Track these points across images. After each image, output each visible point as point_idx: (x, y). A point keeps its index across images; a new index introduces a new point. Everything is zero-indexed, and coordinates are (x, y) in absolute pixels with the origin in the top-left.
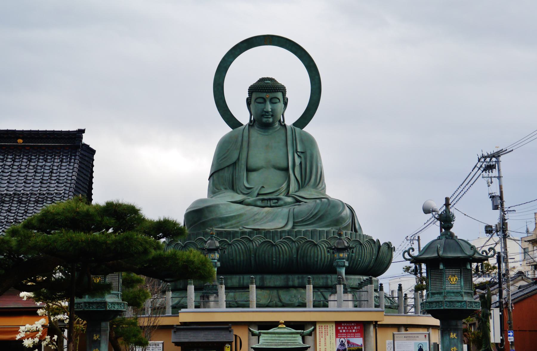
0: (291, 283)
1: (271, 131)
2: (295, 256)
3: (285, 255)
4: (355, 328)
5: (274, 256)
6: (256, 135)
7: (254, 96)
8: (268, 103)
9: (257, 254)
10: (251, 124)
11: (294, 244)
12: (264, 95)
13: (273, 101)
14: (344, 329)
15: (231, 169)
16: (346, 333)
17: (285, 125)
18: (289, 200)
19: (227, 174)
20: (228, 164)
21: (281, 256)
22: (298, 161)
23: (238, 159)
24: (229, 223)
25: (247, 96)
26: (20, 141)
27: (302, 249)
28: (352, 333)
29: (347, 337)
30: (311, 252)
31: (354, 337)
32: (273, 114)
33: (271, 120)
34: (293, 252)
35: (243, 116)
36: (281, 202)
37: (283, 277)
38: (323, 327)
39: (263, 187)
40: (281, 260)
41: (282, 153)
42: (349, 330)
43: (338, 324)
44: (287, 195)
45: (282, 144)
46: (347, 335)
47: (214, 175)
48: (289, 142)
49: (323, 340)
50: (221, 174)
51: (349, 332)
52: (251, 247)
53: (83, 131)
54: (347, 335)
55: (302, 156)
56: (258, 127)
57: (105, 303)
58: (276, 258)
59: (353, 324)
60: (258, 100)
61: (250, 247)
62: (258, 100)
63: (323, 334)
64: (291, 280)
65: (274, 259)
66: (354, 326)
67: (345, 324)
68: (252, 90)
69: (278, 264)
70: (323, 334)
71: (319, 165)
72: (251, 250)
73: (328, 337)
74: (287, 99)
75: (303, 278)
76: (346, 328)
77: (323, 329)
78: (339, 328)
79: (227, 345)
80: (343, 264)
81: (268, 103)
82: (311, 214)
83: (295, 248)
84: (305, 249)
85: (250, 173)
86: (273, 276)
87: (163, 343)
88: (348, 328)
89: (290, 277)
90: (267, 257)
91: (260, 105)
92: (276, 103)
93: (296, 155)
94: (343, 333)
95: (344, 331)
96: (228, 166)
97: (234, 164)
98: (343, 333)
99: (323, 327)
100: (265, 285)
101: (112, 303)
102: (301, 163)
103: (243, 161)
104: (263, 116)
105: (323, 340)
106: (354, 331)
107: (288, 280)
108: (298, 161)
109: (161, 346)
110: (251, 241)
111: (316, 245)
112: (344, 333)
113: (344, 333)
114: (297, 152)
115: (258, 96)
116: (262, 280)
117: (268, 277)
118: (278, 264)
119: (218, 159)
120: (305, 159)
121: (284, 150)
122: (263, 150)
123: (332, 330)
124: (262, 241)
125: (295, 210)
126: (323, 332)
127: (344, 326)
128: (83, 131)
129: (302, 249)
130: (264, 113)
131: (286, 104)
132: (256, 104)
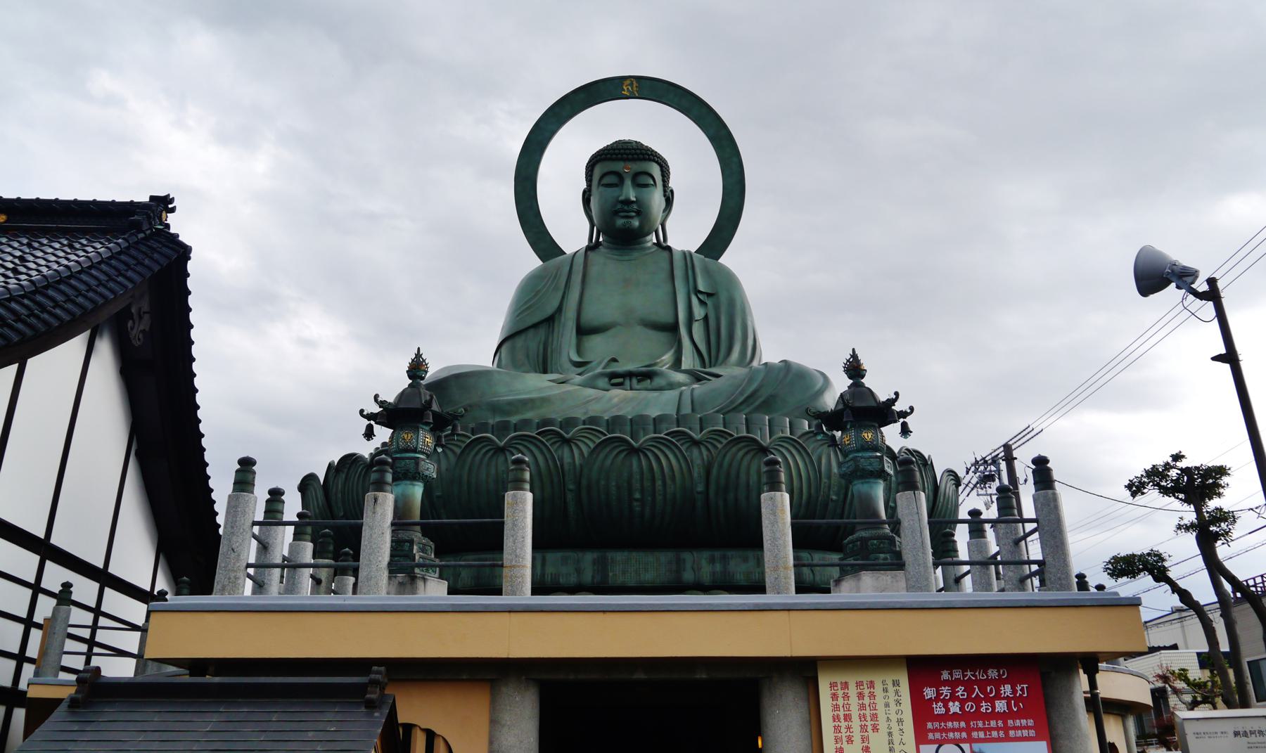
0: (688, 576)
1: (636, 254)
2: (700, 488)
3: (669, 482)
4: (1007, 690)
5: (637, 485)
6: (606, 265)
8: (628, 182)
9: (584, 482)
10: (592, 247)
11: (695, 452)
12: (618, 166)
14: (954, 698)
15: (542, 332)
16: (963, 716)
17: (669, 249)
18: (680, 377)
19: (533, 342)
20: (536, 319)
21: (659, 483)
23: (560, 310)
27: (721, 465)
28: (994, 715)
29: (970, 740)
30: (748, 474)
31: (1008, 739)
32: (641, 210)
33: (636, 223)
34: (695, 475)
36: (658, 381)
37: (665, 557)
38: (853, 691)
39: (614, 360)
40: (659, 498)
41: (662, 293)
42: (977, 701)
43: (923, 669)
45: (663, 276)
46: (969, 730)
47: (504, 349)
48: (679, 273)
50: (519, 342)
51: (978, 715)
52: (567, 459)
53: (163, 204)
54: (969, 730)
55: (709, 302)
56: (608, 248)
58: (642, 491)
59: (993, 673)
60: (605, 181)
61: (561, 460)
62: (606, 180)
63: (856, 723)
64: (688, 565)
65: (637, 496)
66: (998, 683)
67: (957, 674)
69: (647, 510)
70: (856, 723)
71: (749, 323)
72: (566, 467)
74: (672, 192)
75: (724, 559)
76: (960, 691)
77: (854, 701)
78: (929, 693)
80: (876, 466)
81: (628, 182)
82: (741, 394)
83: (698, 461)
84: (728, 474)
85: (585, 338)
86: (634, 554)
88: (969, 690)
89: (687, 556)
90: (613, 490)
91: (610, 190)
92: (646, 186)
93: (695, 301)
94: (947, 717)
95: (955, 707)
96: (535, 326)
97: (550, 321)
98: (947, 717)
99: (853, 691)
100: (611, 582)
102: (706, 318)
106: (1001, 706)
107: (680, 563)
108: (699, 312)
110: (567, 442)
112: (955, 717)
113: (955, 717)
114: (697, 292)
115: (606, 170)
116: (602, 565)
117: (619, 556)
118: (647, 510)
119: (516, 310)
120: (717, 308)
121: (668, 288)
122: (616, 293)
123: (893, 699)
124: (598, 441)
125: (696, 393)
127: (953, 684)
128: (163, 204)
129: (721, 465)
130: (619, 206)
132: (601, 189)
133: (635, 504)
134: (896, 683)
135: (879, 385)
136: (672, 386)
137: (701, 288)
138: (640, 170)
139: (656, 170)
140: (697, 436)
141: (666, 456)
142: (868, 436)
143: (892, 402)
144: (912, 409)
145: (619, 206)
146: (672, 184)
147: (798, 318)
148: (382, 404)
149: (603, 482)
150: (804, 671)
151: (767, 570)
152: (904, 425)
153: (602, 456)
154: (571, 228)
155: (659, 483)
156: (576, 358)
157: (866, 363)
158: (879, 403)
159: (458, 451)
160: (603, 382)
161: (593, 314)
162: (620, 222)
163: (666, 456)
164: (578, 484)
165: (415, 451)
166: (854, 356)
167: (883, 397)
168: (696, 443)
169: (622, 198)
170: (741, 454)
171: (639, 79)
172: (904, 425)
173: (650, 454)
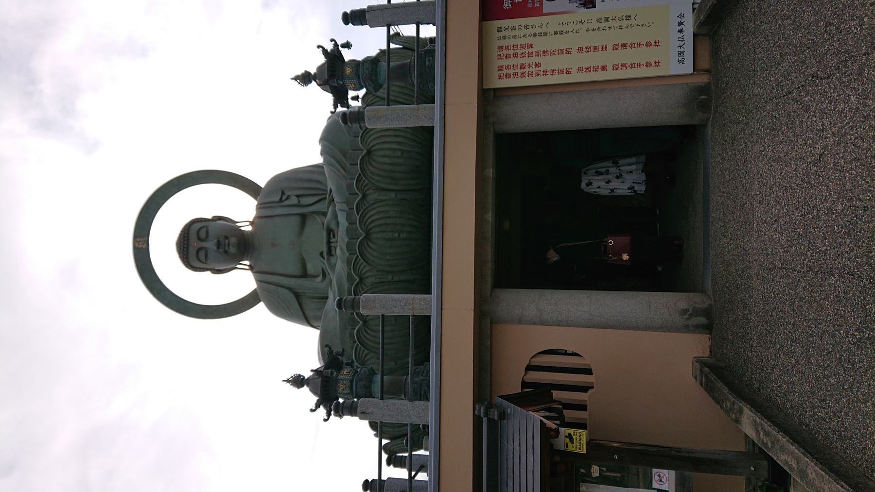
2: (393, 195)
8: (204, 244)
9: (387, 269)
12: (192, 251)
20: (296, 304)
21: (389, 221)
22: (294, 200)
23: (290, 289)
25: (209, 273)
33: (233, 240)
36: (333, 226)
38: (505, 62)
39: (321, 254)
49: (548, 63)
63: (526, 60)
70: (526, 60)
73: (540, 44)
77: (512, 61)
79: (561, 442)
81: (204, 244)
91: (209, 256)
92: (207, 233)
97: (297, 296)
99: (505, 62)
103: (292, 282)
104: (226, 252)
105: (548, 63)
108: (294, 200)
111: (369, 152)
114: (281, 200)
120: (293, 189)
121: (277, 220)
123: (512, 31)
126: (521, 61)
133: (401, 236)
134: (500, 30)
135: (315, 61)
136: (336, 216)
137: (278, 199)
138: (196, 237)
139: (197, 226)
140: (360, 196)
141: (372, 216)
142: (348, 71)
143: (325, 51)
144: (332, 40)
145: (221, 250)
146: (210, 217)
147: (293, 133)
148: (318, 406)
149: (388, 257)
150: (489, 98)
151: (420, 125)
152: (344, 46)
153: (371, 257)
154: (240, 281)
155: (389, 221)
156: (320, 278)
157: (300, 72)
158: (327, 62)
159: (366, 351)
160: (333, 260)
161: (293, 268)
162: (233, 250)
163: (372, 216)
164: (389, 272)
165: (352, 381)
166: (296, 78)
167: (322, 60)
168: (364, 197)
169: (215, 248)
170: (371, 168)
172: (344, 46)
173: (372, 225)
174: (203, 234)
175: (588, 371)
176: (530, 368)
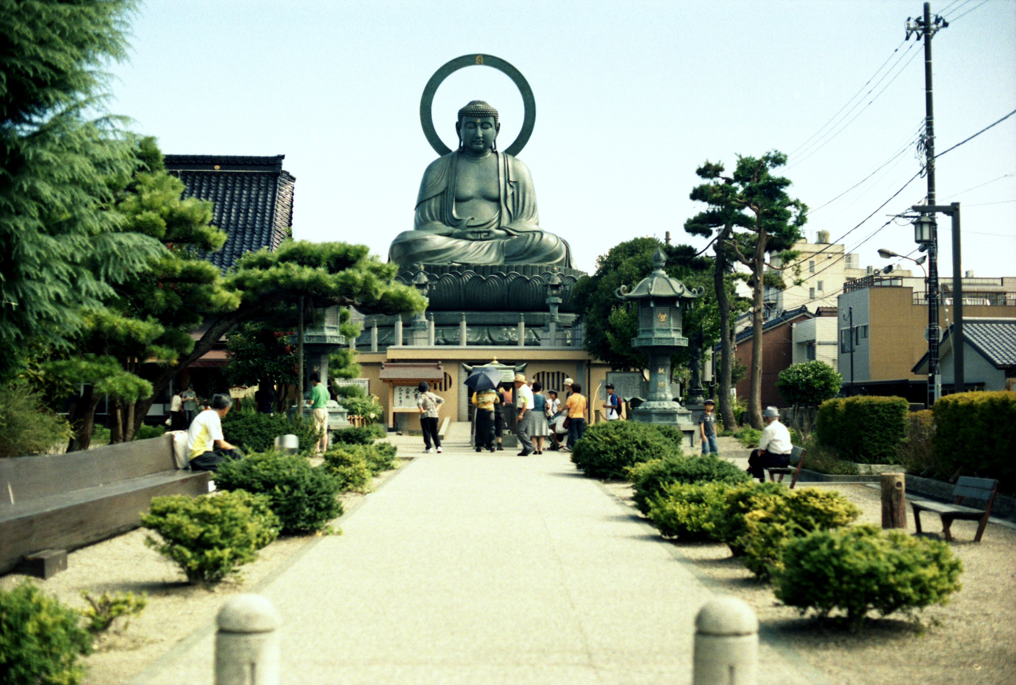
7: (464, 120)
8: (479, 128)
13: (485, 126)
18: (502, 232)
20: (435, 193)
24: (437, 257)
25: (457, 120)
26: (217, 167)
33: (482, 146)
35: (452, 142)
36: (492, 235)
44: (499, 228)
53: (283, 157)
57: (325, 337)
60: (468, 125)
68: (463, 114)
81: (479, 128)
87: (369, 381)
96: (436, 196)
101: (332, 337)
102: (513, 194)
108: (510, 192)
109: (367, 383)
114: (509, 181)
128: (283, 157)
131: (497, 129)
139: (491, 120)
171: (485, 56)
174: (485, 125)
175: (446, 390)
176: (445, 374)
